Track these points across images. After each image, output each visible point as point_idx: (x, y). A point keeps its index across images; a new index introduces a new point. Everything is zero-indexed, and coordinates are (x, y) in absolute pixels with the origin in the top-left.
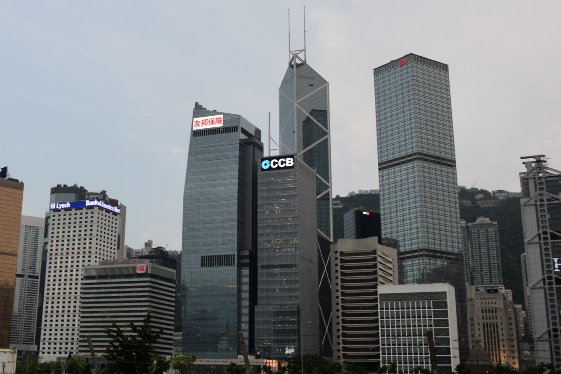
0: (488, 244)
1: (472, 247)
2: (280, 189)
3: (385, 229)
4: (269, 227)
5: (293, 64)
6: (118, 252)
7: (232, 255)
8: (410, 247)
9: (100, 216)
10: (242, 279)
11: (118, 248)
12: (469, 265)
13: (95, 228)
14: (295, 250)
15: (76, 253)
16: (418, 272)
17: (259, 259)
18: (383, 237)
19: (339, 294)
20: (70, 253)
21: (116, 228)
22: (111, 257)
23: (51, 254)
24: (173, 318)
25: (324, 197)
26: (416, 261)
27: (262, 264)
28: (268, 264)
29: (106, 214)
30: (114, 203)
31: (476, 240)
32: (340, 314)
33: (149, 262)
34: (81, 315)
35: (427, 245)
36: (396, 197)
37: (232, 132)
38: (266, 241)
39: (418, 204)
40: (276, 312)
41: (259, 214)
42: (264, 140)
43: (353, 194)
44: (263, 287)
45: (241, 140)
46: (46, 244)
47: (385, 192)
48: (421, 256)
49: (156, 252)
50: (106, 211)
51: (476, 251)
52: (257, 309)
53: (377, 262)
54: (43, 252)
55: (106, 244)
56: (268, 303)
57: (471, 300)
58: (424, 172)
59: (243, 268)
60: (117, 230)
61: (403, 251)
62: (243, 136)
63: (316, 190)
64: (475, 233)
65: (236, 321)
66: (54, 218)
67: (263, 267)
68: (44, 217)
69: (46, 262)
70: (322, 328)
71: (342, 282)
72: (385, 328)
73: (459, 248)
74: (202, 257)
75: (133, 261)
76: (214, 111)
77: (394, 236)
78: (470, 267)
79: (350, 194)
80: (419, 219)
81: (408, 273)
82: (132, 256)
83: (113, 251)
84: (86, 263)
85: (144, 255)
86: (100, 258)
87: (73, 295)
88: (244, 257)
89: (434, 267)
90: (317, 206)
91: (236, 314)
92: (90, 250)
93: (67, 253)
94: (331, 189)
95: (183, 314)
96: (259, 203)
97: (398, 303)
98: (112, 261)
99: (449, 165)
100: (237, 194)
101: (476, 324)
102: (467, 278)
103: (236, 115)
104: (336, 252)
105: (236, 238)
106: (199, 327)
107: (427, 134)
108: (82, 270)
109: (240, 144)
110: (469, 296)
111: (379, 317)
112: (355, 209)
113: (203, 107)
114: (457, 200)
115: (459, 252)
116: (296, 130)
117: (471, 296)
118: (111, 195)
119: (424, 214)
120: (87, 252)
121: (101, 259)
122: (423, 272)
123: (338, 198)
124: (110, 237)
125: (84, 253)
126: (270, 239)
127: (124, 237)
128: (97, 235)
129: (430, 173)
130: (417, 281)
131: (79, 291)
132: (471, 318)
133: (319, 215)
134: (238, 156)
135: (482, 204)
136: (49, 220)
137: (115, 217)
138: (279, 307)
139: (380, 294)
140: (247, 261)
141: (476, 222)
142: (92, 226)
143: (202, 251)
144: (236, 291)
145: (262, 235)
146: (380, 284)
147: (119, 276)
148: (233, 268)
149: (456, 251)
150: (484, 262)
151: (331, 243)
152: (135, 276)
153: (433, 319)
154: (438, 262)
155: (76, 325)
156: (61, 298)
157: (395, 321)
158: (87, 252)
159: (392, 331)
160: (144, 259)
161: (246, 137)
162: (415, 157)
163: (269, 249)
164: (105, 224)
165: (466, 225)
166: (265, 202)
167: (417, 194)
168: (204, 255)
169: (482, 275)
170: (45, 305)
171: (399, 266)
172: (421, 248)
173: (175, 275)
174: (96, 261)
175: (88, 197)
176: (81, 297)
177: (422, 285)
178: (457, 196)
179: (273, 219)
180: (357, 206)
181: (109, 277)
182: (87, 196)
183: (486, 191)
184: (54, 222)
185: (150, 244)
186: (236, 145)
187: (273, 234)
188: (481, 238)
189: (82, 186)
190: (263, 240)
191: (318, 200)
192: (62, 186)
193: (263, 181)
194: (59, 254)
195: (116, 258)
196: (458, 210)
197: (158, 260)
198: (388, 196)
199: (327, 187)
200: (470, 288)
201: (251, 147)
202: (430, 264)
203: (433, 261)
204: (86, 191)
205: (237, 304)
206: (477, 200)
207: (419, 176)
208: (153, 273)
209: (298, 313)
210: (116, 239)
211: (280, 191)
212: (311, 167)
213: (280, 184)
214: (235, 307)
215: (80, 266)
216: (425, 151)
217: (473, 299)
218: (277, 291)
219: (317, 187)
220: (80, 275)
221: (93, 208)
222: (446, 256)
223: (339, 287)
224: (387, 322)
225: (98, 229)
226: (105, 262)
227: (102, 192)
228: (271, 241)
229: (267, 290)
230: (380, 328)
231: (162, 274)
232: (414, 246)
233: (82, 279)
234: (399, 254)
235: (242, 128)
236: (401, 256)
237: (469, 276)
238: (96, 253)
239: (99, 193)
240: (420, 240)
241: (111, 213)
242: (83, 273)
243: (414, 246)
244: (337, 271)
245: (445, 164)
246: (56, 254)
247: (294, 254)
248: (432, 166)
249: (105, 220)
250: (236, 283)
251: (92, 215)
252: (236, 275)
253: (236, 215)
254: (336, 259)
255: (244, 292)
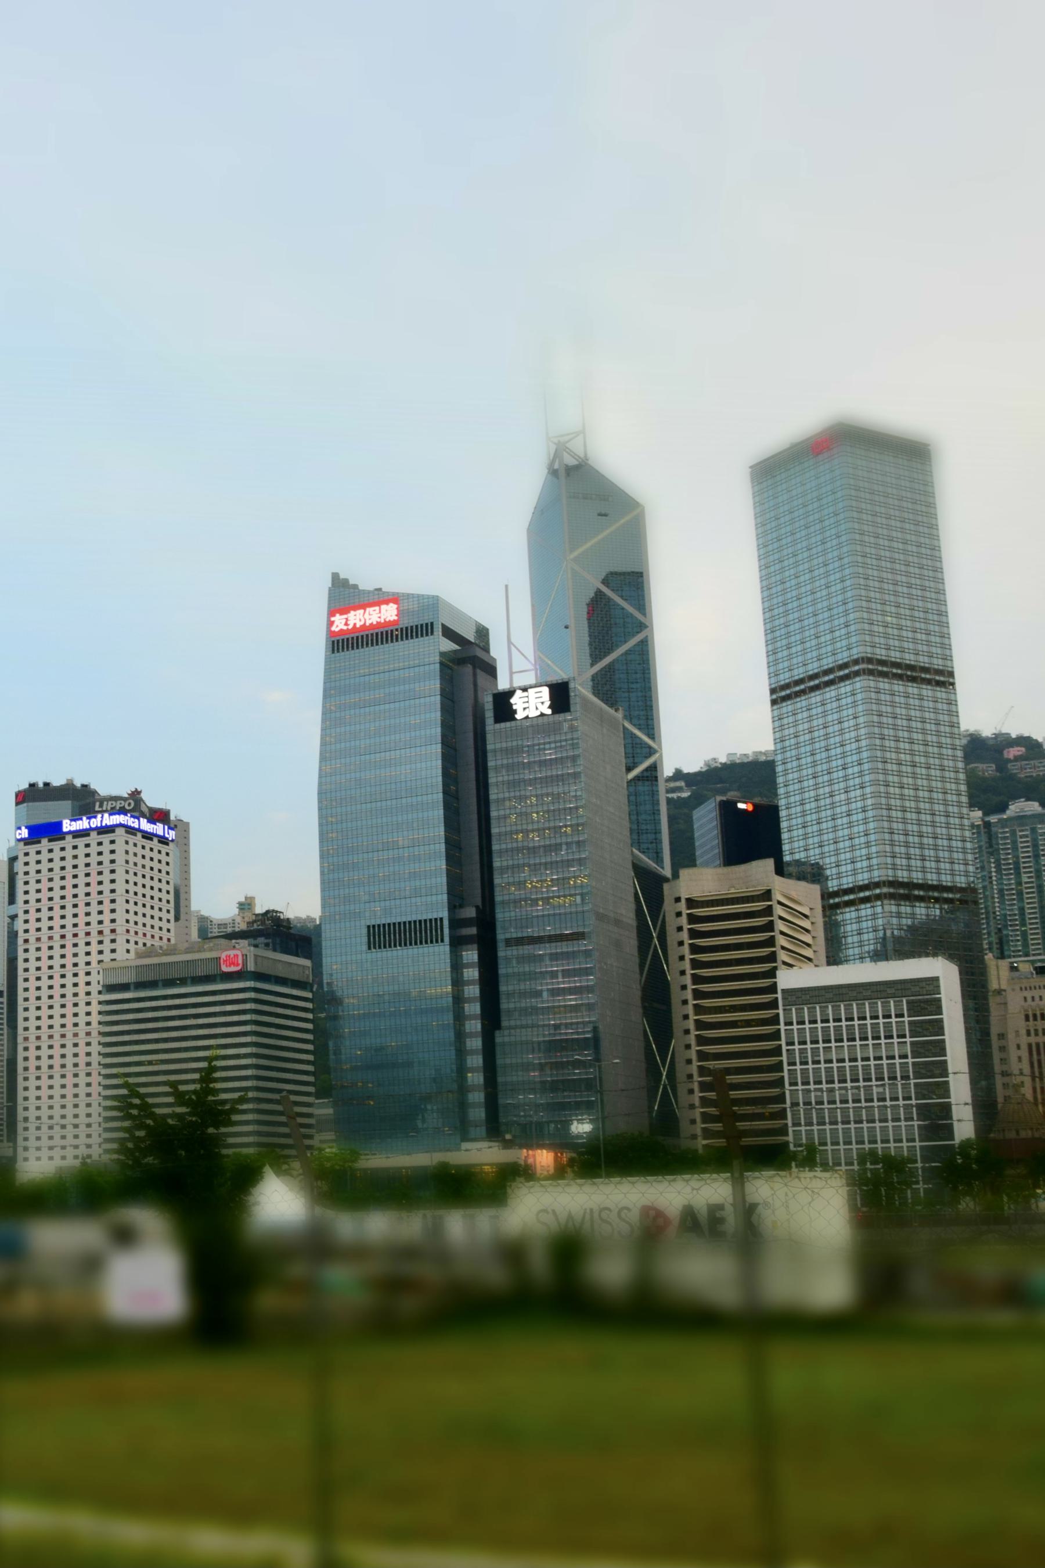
0: (1037, 862)
1: (999, 870)
2: (540, 761)
3: (791, 840)
4: (518, 850)
5: (556, 466)
6: (175, 927)
7: (436, 919)
8: (850, 879)
9: (131, 849)
10: (462, 973)
11: (177, 918)
12: (994, 913)
13: (120, 876)
14: (583, 900)
15: (82, 934)
16: (871, 936)
17: (499, 925)
18: (787, 858)
19: (689, 995)
20: (69, 936)
21: (168, 873)
22: (161, 938)
23: (26, 941)
24: (311, 1068)
25: (645, 774)
26: (866, 910)
27: (508, 936)
28: (520, 935)
29: (145, 842)
30: (160, 816)
31: (1009, 854)
32: (692, 1039)
33: (249, 945)
34: (104, 1071)
35: (890, 872)
36: (814, 764)
37: (422, 636)
38: (514, 884)
39: (867, 778)
40: (544, 1041)
41: (494, 823)
42: (498, 651)
43: (714, 765)
44: (511, 988)
45: (442, 654)
46: (13, 917)
47: (788, 754)
48: (878, 897)
49: (263, 923)
50: (143, 837)
51: (1009, 879)
52: (500, 1038)
53: (775, 918)
54: (9, 937)
55: (148, 911)
56: (524, 1023)
57: (999, 992)
58: (878, 702)
59: (464, 947)
60: (170, 878)
61: (836, 889)
62: (448, 646)
63: (624, 760)
64: (1006, 838)
65: (454, 1067)
66: (27, 859)
67: (509, 942)
68: (6, 859)
69: (16, 959)
70: (653, 1071)
71: (693, 968)
72: (798, 1067)
73: (966, 874)
74: (369, 927)
75: (212, 945)
76: (376, 590)
77: (814, 856)
78: (995, 918)
79: (707, 764)
80: (870, 814)
81: (850, 940)
82: (210, 935)
83: (164, 925)
84: (107, 956)
85: (237, 929)
86: (136, 943)
87: (82, 1029)
88: (466, 923)
89: (909, 922)
90: (629, 796)
91: (453, 1052)
92: (113, 926)
93: (63, 937)
94: (661, 756)
95: (332, 1057)
96: (493, 797)
97: (827, 1007)
98: (165, 947)
99: (939, 684)
100: (440, 779)
101: (1012, 1048)
102: (990, 943)
103: (429, 597)
104: (678, 900)
105: (444, 879)
106: (370, 1085)
107: (884, 613)
108: (99, 972)
109: (441, 664)
110: (994, 985)
111: (783, 1042)
112: (719, 798)
113: (351, 582)
114: (961, 765)
115: (969, 884)
116: (572, 624)
117: (999, 984)
118: (152, 800)
119: (883, 801)
120: (107, 931)
121: (140, 944)
122: (885, 934)
123: (678, 775)
124: (156, 894)
125: (100, 933)
126: (522, 879)
127: (188, 893)
128: (127, 891)
129: (893, 704)
130: (870, 957)
131: (95, 1018)
132: (999, 1035)
133: (634, 817)
134: (439, 693)
135: (1022, 768)
136: (15, 864)
137: (164, 849)
138: (552, 1032)
139: (782, 990)
140: (473, 931)
141: (1008, 812)
142: (113, 871)
143: (367, 914)
144: (450, 999)
145: (503, 870)
146: (784, 967)
147: (183, 982)
148: (442, 948)
149: (961, 881)
150: (1028, 903)
151: (667, 880)
152: (218, 978)
153: (908, 1040)
154: (918, 910)
155: (95, 1095)
156: (57, 1037)
157: (821, 1050)
158: (107, 931)
159: (814, 1073)
160: (236, 938)
161: (456, 647)
162: (856, 668)
163: (521, 900)
164: (144, 866)
165: (983, 820)
166: (507, 795)
167: (865, 755)
168: (373, 923)
169: (1024, 934)
170: (21, 1054)
171: (825, 924)
172: (877, 880)
173: (309, 973)
174: (128, 951)
175: (101, 806)
176: (100, 1033)
177: (882, 964)
178: (960, 754)
179: (526, 832)
180: (723, 792)
181: (160, 984)
182: (97, 804)
183: (1029, 738)
184: (26, 869)
185: (249, 904)
186: (432, 667)
187: (529, 866)
188: (1020, 850)
189: (85, 783)
190: (506, 880)
191: (629, 782)
192: (41, 785)
193: (498, 746)
194: (44, 938)
195: (173, 941)
196: (963, 788)
197: (270, 941)
198: (795, 764)
199: (651, 752)
200: (998, 967)
201: (468, 669)
202: (899, 915)
203: (905, 909)
204: (94, 793)
205: (455, 1029)
206: (1009, 761)
207: (869, 712)
208: (258, 971)
209: (595, 1043)
210: (171, 897)
211: (540, 766)
212: (611, 706)
213: (539, 750)
214: (451, 1035)
215: (94, 964)
216: (881, 653)
217: (1005, 991)
218: (545, 994)
219: (625, 753)
220: (94, 983)
221: (113, 831)
222: (936, 894)
223: (688, 980)
224: (803, 1052)
225: (127, 877)
226: (150, 952)
227: (133, 793)
228: (525, 882)
229: (523, 994)
230: (786, 1067)
231: (281, 972)
232: (860, 877)
233: (100, 992)
234: (826, 895)
235: (443, 625)
236: (831, 901)
237: (994, 939)
238: (128, 931)
239: (127, 796)
240: (874, 861)
241: (155, 840)
242: (100, 978)
243: (860, 877)
244: (681, 943)
245: (929, 682)
246: (38, 939)
247: (580, 909)
248: (898, 687)
249: (143, 857)
250: (449, 982)
251: (113, 847)
252: (449, 965)
253: (442, 829)
254: (679, 914)
255: (470, 1000)
